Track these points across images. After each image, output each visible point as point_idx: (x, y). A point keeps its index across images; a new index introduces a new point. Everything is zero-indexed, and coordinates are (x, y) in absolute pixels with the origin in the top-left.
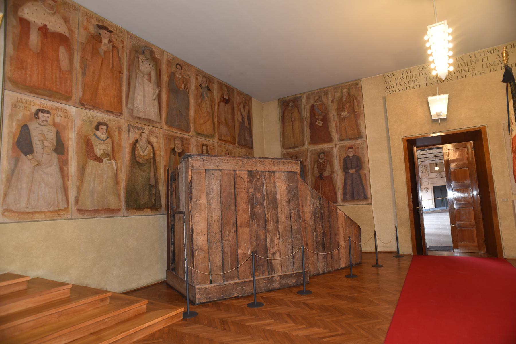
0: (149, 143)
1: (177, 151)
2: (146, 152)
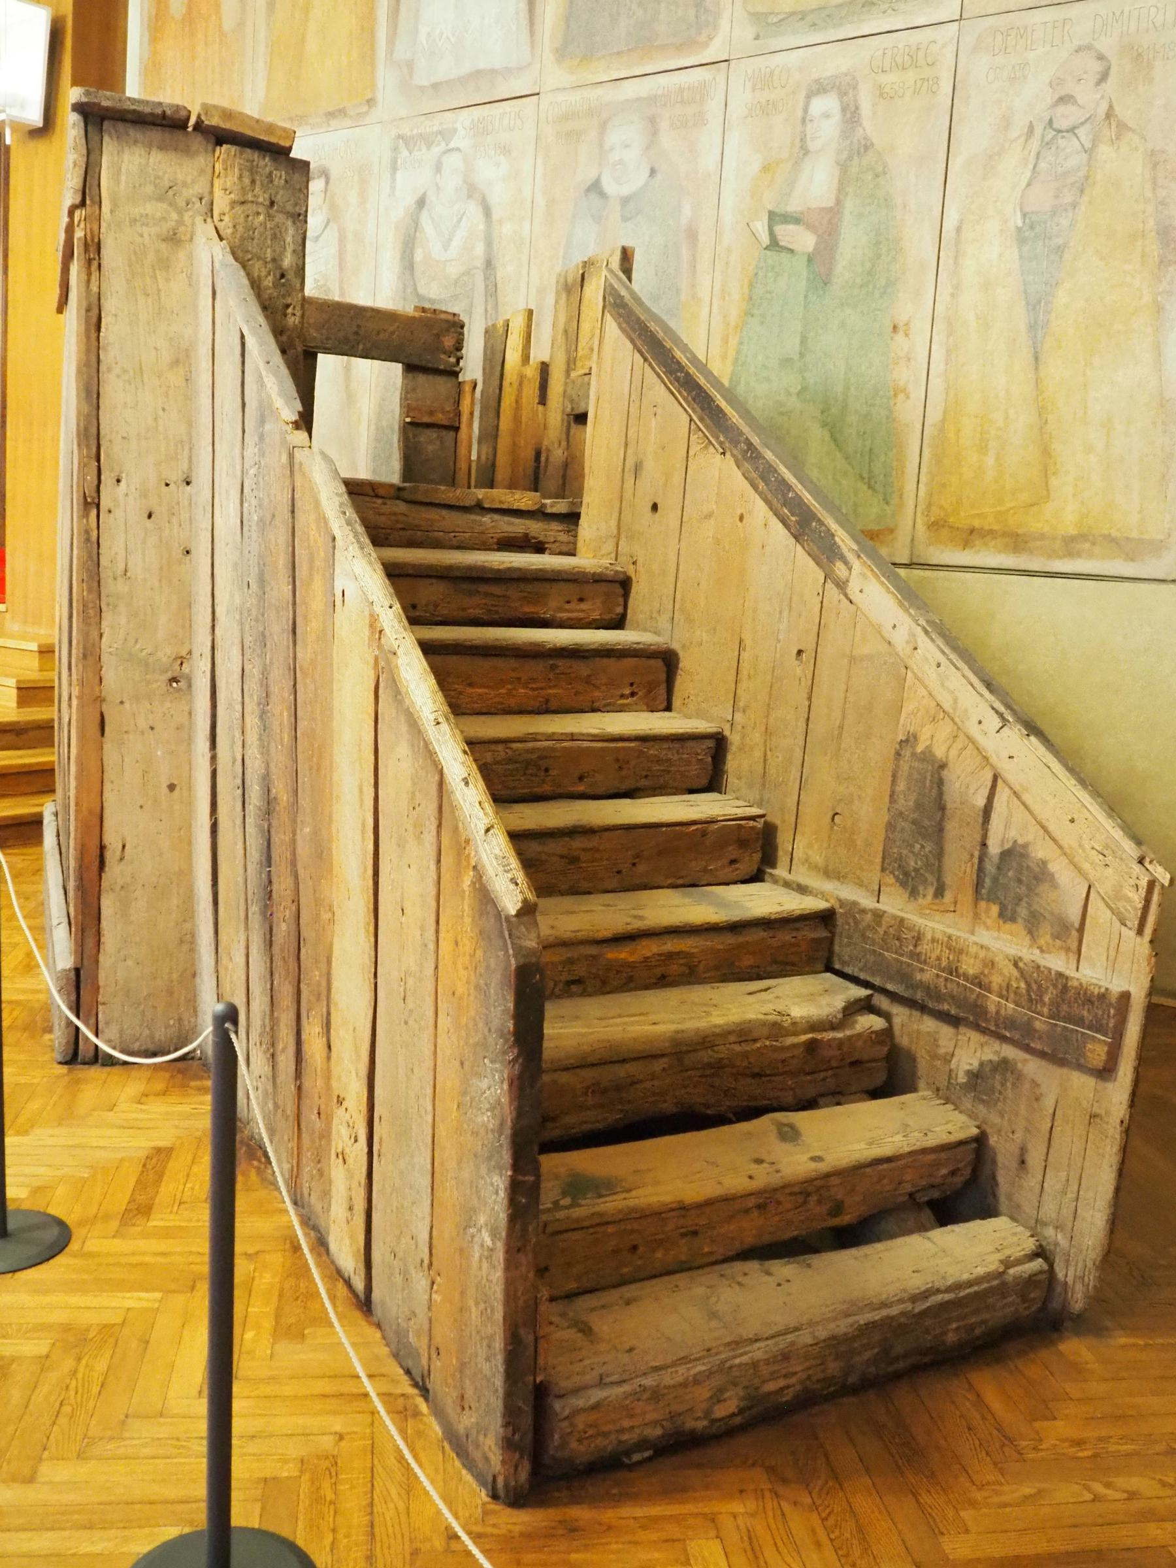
0: (471, 189)
1: (608, 186)
2: (457, 242)
